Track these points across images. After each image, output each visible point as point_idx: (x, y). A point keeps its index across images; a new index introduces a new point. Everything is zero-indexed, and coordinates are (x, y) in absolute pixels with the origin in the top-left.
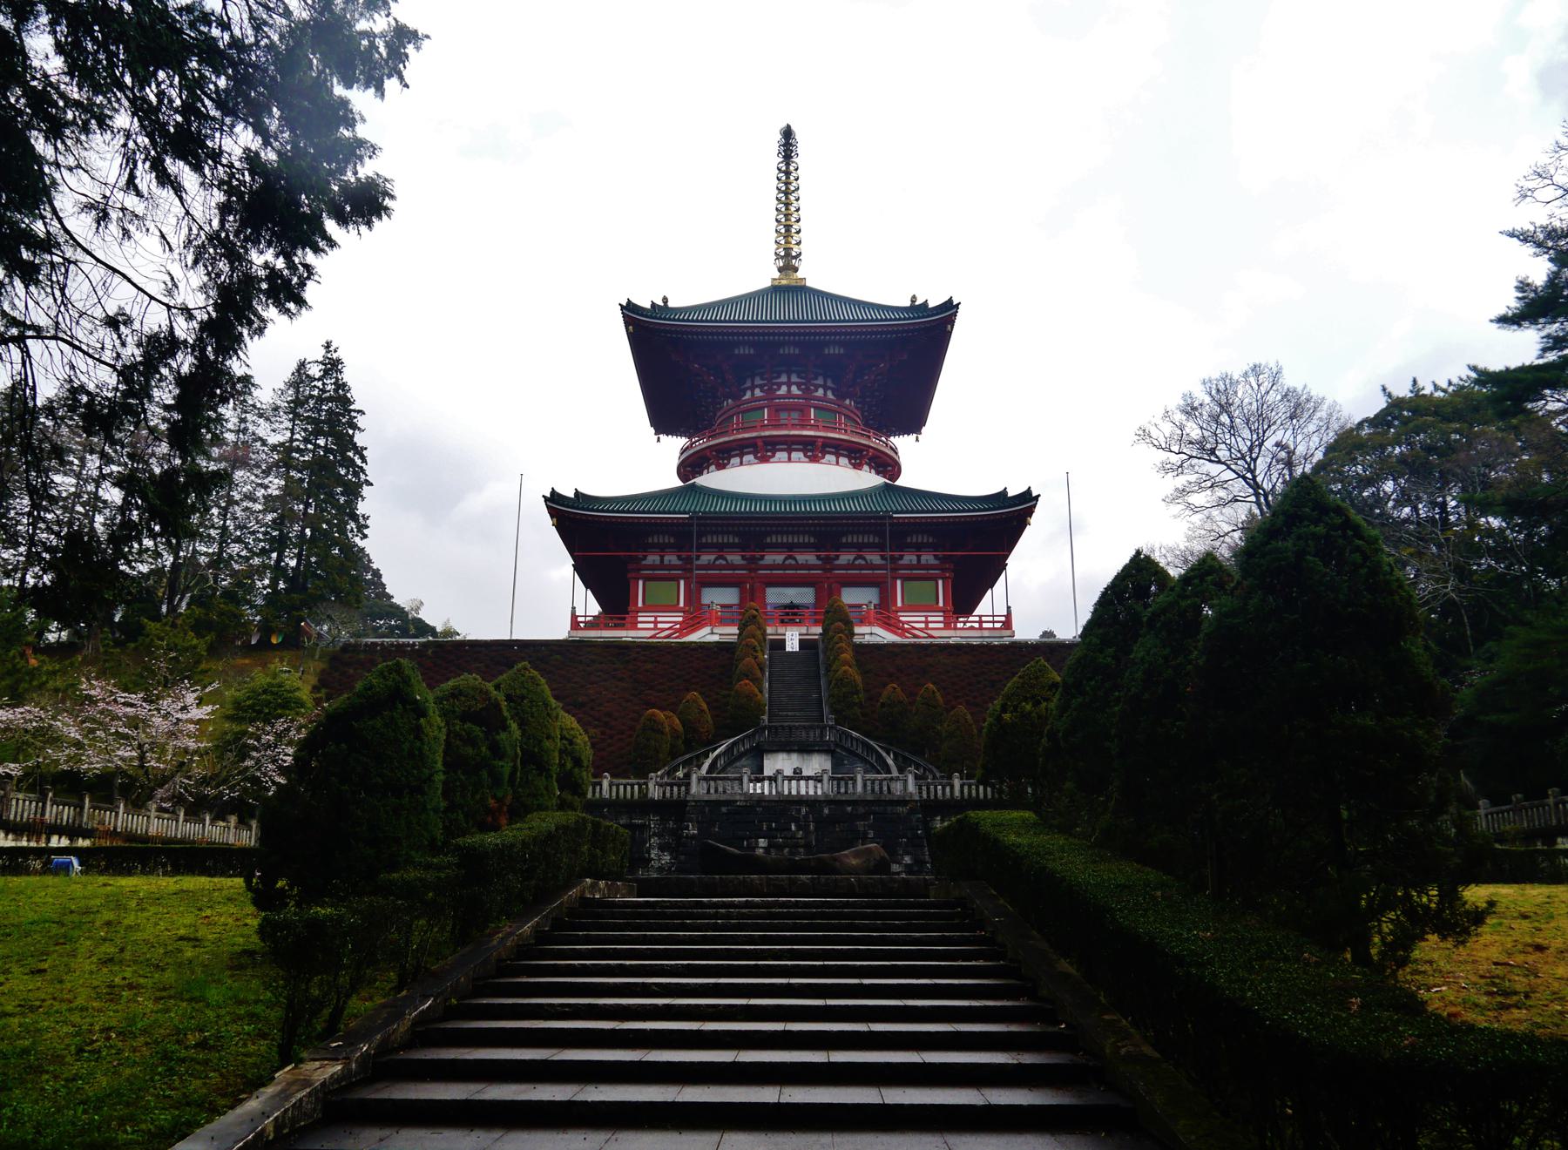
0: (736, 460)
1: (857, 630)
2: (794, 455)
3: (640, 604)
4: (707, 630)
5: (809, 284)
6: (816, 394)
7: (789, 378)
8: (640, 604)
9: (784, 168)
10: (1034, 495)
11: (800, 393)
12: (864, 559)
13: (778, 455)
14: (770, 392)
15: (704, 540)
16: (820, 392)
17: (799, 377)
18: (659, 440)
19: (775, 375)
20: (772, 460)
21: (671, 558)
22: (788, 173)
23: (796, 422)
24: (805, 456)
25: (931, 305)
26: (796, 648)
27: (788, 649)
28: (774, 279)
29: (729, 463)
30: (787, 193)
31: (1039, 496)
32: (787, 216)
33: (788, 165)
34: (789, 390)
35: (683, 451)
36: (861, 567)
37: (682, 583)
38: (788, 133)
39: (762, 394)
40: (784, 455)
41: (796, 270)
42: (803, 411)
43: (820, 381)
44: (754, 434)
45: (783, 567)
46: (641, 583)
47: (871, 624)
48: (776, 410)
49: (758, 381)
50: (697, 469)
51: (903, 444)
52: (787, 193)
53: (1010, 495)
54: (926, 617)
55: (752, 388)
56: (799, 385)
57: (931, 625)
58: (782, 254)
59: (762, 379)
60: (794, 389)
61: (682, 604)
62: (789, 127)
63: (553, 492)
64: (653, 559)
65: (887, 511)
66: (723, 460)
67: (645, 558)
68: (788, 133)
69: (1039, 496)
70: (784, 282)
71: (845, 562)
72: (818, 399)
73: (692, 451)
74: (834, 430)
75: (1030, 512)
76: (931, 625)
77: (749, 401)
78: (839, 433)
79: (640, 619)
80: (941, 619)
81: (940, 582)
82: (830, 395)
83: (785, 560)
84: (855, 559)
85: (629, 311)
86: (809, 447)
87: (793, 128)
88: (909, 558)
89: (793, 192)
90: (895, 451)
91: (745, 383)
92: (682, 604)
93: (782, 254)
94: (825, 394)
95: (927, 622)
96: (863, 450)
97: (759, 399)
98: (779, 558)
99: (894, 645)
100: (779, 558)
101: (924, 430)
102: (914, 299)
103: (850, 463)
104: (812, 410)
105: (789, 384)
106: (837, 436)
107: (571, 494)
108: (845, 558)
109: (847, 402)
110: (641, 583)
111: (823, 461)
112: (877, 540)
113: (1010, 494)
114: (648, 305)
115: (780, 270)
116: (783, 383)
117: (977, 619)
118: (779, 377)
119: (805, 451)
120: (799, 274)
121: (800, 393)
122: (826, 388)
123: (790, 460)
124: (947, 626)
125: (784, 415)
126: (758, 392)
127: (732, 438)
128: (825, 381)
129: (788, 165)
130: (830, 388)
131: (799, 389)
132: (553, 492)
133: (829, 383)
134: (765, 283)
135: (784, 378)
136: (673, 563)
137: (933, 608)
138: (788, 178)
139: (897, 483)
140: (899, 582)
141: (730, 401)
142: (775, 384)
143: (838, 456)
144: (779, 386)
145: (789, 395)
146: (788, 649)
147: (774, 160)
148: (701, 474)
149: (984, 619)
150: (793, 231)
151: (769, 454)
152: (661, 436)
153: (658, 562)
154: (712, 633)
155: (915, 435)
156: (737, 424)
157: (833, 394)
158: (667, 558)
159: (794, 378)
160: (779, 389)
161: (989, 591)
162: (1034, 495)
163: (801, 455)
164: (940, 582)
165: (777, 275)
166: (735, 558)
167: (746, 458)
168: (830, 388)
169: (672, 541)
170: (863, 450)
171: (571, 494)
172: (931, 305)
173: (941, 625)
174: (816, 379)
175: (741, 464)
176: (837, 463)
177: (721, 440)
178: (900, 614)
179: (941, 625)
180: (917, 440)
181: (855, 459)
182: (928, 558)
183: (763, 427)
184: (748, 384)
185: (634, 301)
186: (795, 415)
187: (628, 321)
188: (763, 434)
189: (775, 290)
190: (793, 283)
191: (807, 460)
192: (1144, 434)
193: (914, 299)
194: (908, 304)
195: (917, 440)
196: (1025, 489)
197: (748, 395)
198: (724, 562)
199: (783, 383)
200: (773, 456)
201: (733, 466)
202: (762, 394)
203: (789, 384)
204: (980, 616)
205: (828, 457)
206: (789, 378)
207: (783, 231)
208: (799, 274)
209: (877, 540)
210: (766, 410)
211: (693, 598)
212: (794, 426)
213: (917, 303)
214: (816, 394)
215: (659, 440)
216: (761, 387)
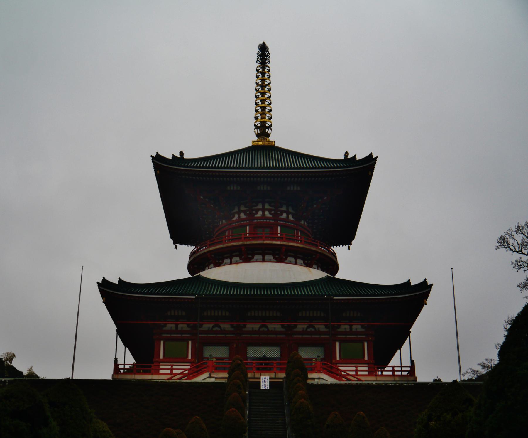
0: (228, 260)
1: (310, 375)
3: (161, 357)
4: (206, 375)
5: (277, 144)
6: (281, 217)
7: (263, 206)
8: (161, 357)
9: (261, 70)
10: (428, 284)
11: (270, 216)
12: (314, 327)
13: (256, 257)
14: (251, 216)
15: (205, 314)
16: (284, 216)
17: (270, 206)
18: (176, 248)
20: (252, 260)
21: (182, 326)
22: (263, 74)
23: (268, 235)
24: (274, 258)
25: (358, 158)
26: (268, 387)
27: (262, 388)
28: (254, 142)
29: (222, 262)
30: (263, 86)
31: (432, 285)
32: (263, 101)
33: (263, 68)
35: (192, 254)
36: (311, 333)
37: (190, 343)
38: (263, 48)
39: (245, 217)
41: (268, 135)
42: (272, 227)
43: (284, 208)
44: (240, 243)
45: (258, 332)
46: (162, 343)
47: (319, 372)
48: (255, 227)
49: (243, 208)
51: (340, 251)
52: (263, 86)
53: (412, 284)
54: (356, 367)
55: (239, 213)
56: (270, 211)
57: (359, 373)
58: (259, 125)
59: (245, 207)
60: (267, 213)
61: (190, 357)
62: (264, 44)
63: (104, 280)
64: (171, 326)
65: (329, 295)
67: (165, 325)
68: (263, 48)
69: (432, 285)
70: (260, 143)
71: (301, 330)
72: (283, 220)
73: (198, 254)
74: (293, 240)
75: (426, 295)
76: (359, 373)
78: (297, 243)
79: (161, 367)
80: (366, 368)
81: (366, 344)
83: (260, 328)
84: (308, 327)
85: (157, 160)
87: (267, 44)
88: (345, 327)
89: (267, 85)
90: (334, 255)
92: (190, 357)
93: (259, 125)
94: (288, 217)
95: (357, 371)
97: (244, 220)
98: (256, 327)
99: (332, 385)
100: (256, 327)
101: (353, 242)
102: (347, 154)
103: (304, 263)
104: (279, 228)
105: (263, 210)
106: (295, 245)
107: (116, 282)
108: (301, 327)
109: (302, 222)
110: (162, 343)
111: (286, 261)
112: (322, 315)
113: (413, 284)
114: (170, 157)
115: (258, 135)
116: (260, 210)
117: (391, 369)
118: (257, 205)
120: (271, 139)
121: (270, 216)
122: (288, 213)
123: (263, 261)
124: (371, 373)
125: (260, 230)
126: (242, 215)
127: (225, 245)
128: (288, 209)
129: (263, 68)
130: (291, 213)
131: (270, 213)
132: (104, 280)
133: (290, 210)
134: (250, 144)
135: (260, 206)
136: (184, 329)
137: (361, 361)
138: (263, 76)
139: (336, 276)
140: (337, 344)
141: (224, 221)
142: (255, 210)
144: (257, 211)
145: (263, 217)
146: (262, 388)
147: (255, 65)
148: (204, 270)
149: (396, 369)
150: (267, 110)
151: (250, 256)
152: (178, 245)
153: (174, 329)
154: (210, 377)
155: (347, 246)
156: (229, 236)
157: (293, 217)
158: (180, 326)
159: (267, 206)
160: (257, 213)
161: (399, 351)
162: (428, 284)
163: (271, 257)
164: (366, 344)
165: (256, 139)
166: (226, 326)
167: (234, 259)
168: (291, 213)
169: (184, 314)
171: (116, 282)
172: (358, 158)
173: (367, 373)
174: (282, 207)
175: (231, 263)
177: (218, 247)
178: (338, 365)
179: (367, 373)
180: (349, 249)
182: (357, 327)
183: (246, 238)
184: (236, 210)
185: (161, 154)
186: (267, 230)
187: (156, 167)
188: (246, 243)
189: (253, 149)
190: (266, 144)
191: (275, 260)
192: (503, 242)
193: (347, 154)
194: (342, 157)
195: (349, 249)
196: (422, 280)
197: (236, 217)
198: (219, 329)
199: (260, 210)
200: (253, 258)
201: (226, 264)
202: (245, 217)
203: (263, 210)
204: (393, 367)
205: (289, 259)
206: (263, 206)
207: (260, 110)
208: (271, 139)
209: (322, 315)
210: (248, 228)
211: (198, 354)
212: (267, 238)
213: (349, 157)
214: (281, 217)
215: (176, 248)
216: (245, 212)
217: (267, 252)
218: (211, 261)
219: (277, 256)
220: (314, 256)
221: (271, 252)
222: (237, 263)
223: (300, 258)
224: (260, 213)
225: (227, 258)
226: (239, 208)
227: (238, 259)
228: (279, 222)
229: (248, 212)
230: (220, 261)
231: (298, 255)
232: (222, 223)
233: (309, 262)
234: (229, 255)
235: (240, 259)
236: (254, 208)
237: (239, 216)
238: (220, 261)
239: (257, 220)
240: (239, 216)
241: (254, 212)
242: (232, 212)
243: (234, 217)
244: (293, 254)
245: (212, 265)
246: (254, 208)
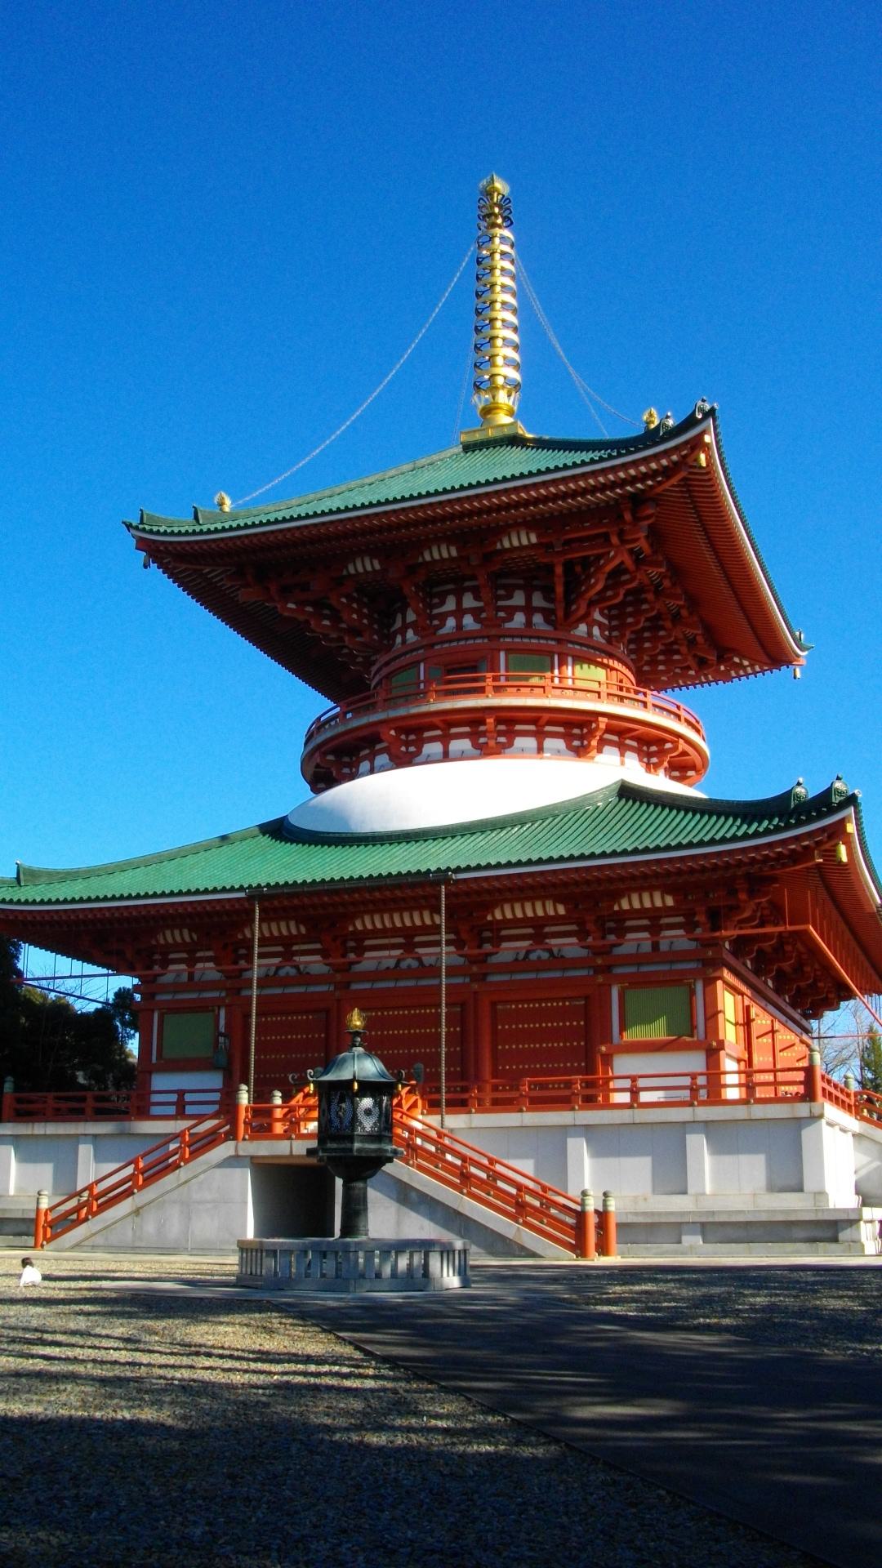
0: (435, 748)
2: (549, 743)
13: (520, 742)
19: (501, 592)
24: (570, 747)
34: (529, 623)
35: (319, 725)
39: (477, 627)
40: (531, 742)
49: (469, 601)
50: (346, 759)
55: (459, 613)
59: (477, 598)
66: (407, 744)
77: (448, 639)
82: (596, 631)
86: (576, 731)
91: (443, 603)
96: (666, 741)
97: (472, 635)
118: (510, 597)
119: (567, 737)
126: (468, 620)
130: (600, 625)
131: (547, 621)
135: (519, 599)
143: (623, 748)
144: (511, 611)
151: (502, 739)
157: (602, 634)
159: (538, 600)
160: (510, 618)
163: (560, 744)
167: (457, 745)
168: (600, 625)
170: (666, 741)
175: (446, 757)
176: (623, 763)
181: (650, 755)
184: (450, 604)
200: (510, 744)
203: (529, 610)
206: (529, 599)
216: (475, 612)
217: (548, 728)
218: (378, 747)
219: (576, 743)
220: (668, 746)
221: (561, 729)
222: (462, 757)
223: (631, 749)
224: (519, 619)
225: (432, 739)
226: (459, 602)
227: (464, 744)
228: (570, 645)
229: (484, 615)
230: (412, 749)
231: (628, 742)
232: (404, 641)
233: (654, 760)
234: (439, 732)
235: (476, 745)
236: (500, 603)
237: (459, 626)
238: (412, 749)
239: (513, 637)
240: (459, 626)
241: (502, 614)
242: (436, 611)
243: (443, 625)
244: (615, 738)
245: (382, 759)
246: (500, 603)
